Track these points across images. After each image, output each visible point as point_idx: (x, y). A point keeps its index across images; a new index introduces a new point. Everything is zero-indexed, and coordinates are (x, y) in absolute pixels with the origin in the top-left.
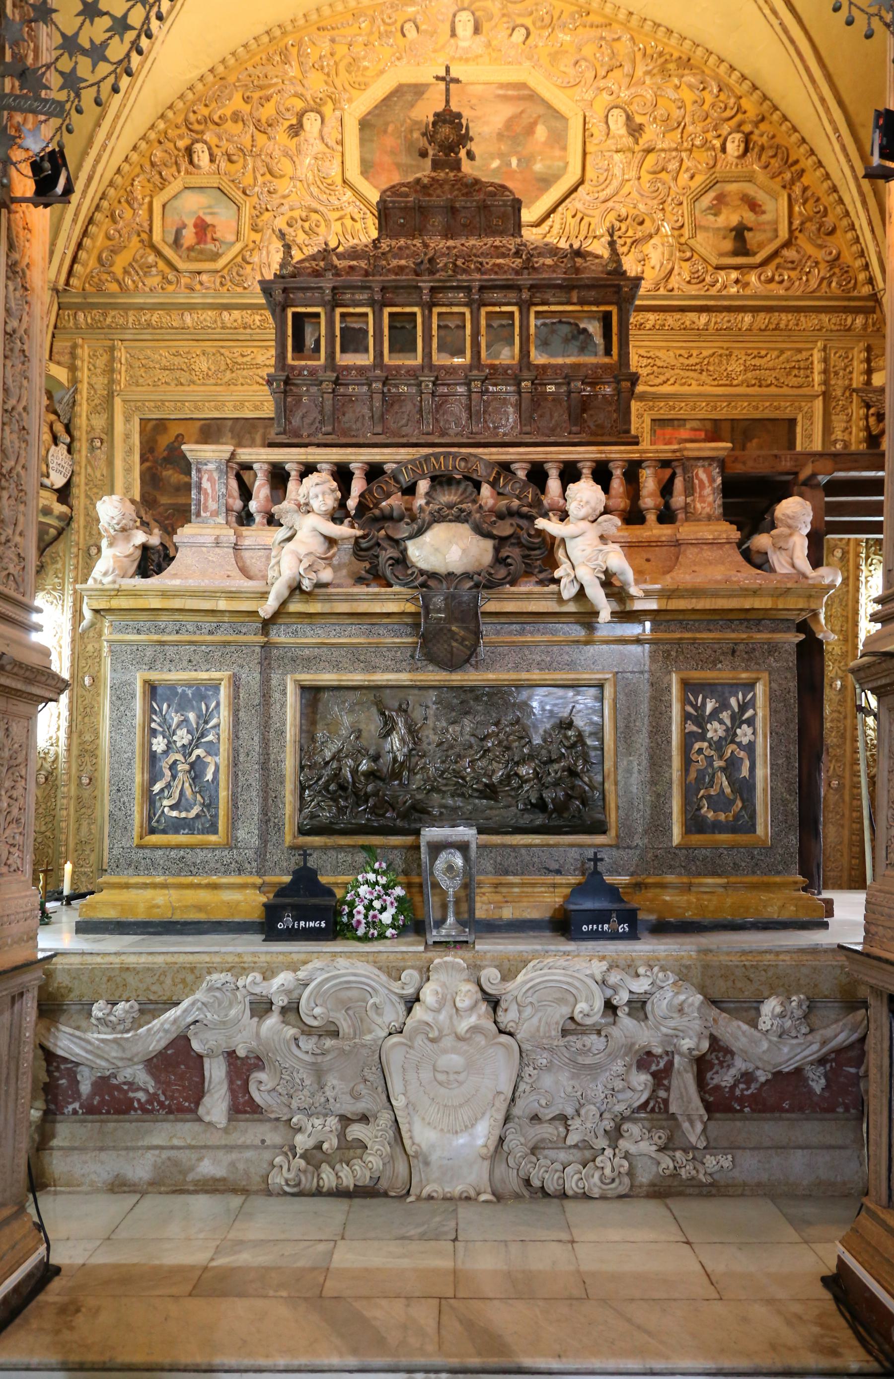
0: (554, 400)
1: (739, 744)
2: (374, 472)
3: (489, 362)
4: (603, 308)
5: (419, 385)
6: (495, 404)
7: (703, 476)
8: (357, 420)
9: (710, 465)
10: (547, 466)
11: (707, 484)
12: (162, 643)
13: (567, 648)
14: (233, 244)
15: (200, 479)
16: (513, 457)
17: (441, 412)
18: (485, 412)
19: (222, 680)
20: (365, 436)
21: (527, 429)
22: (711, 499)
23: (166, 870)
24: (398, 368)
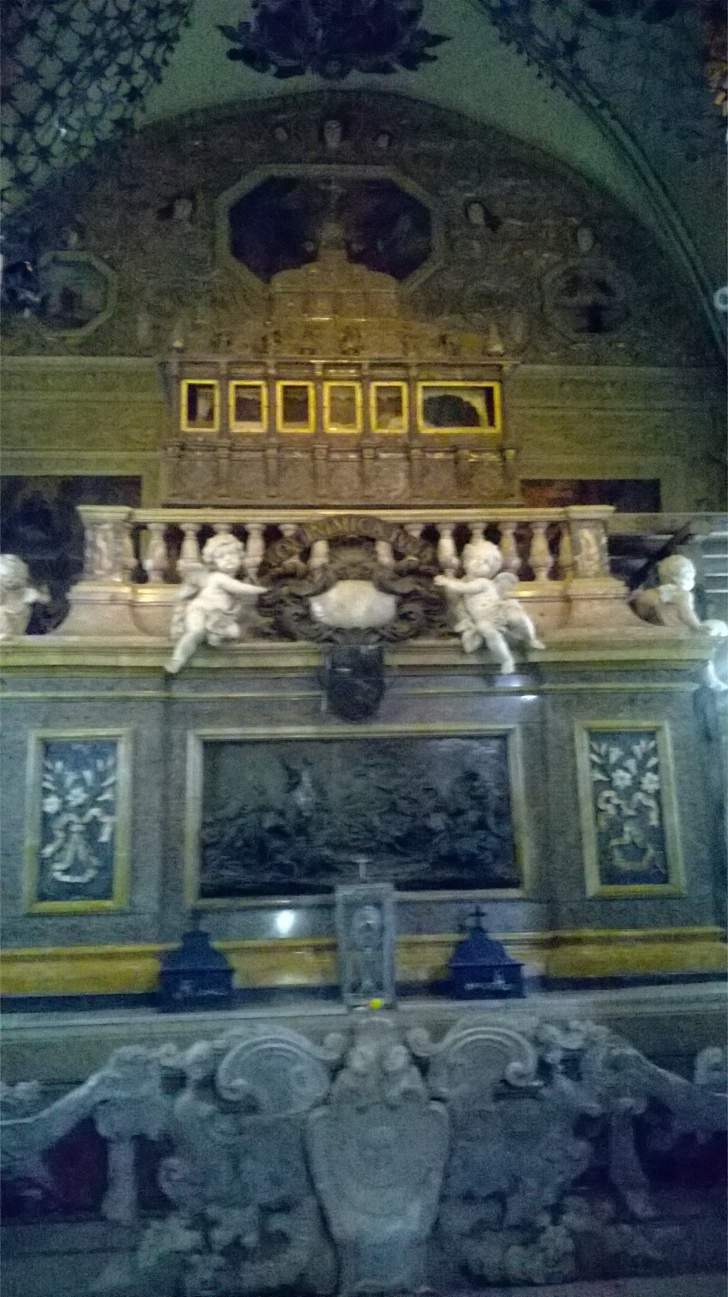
1: (646, 792)
2: (272, 534)
5: (313, 451)
10: (439, 527)
15: (95, 537)
16: (407, 519)
19: (120, 736)
22: (597, 557)
23: (56, 942)
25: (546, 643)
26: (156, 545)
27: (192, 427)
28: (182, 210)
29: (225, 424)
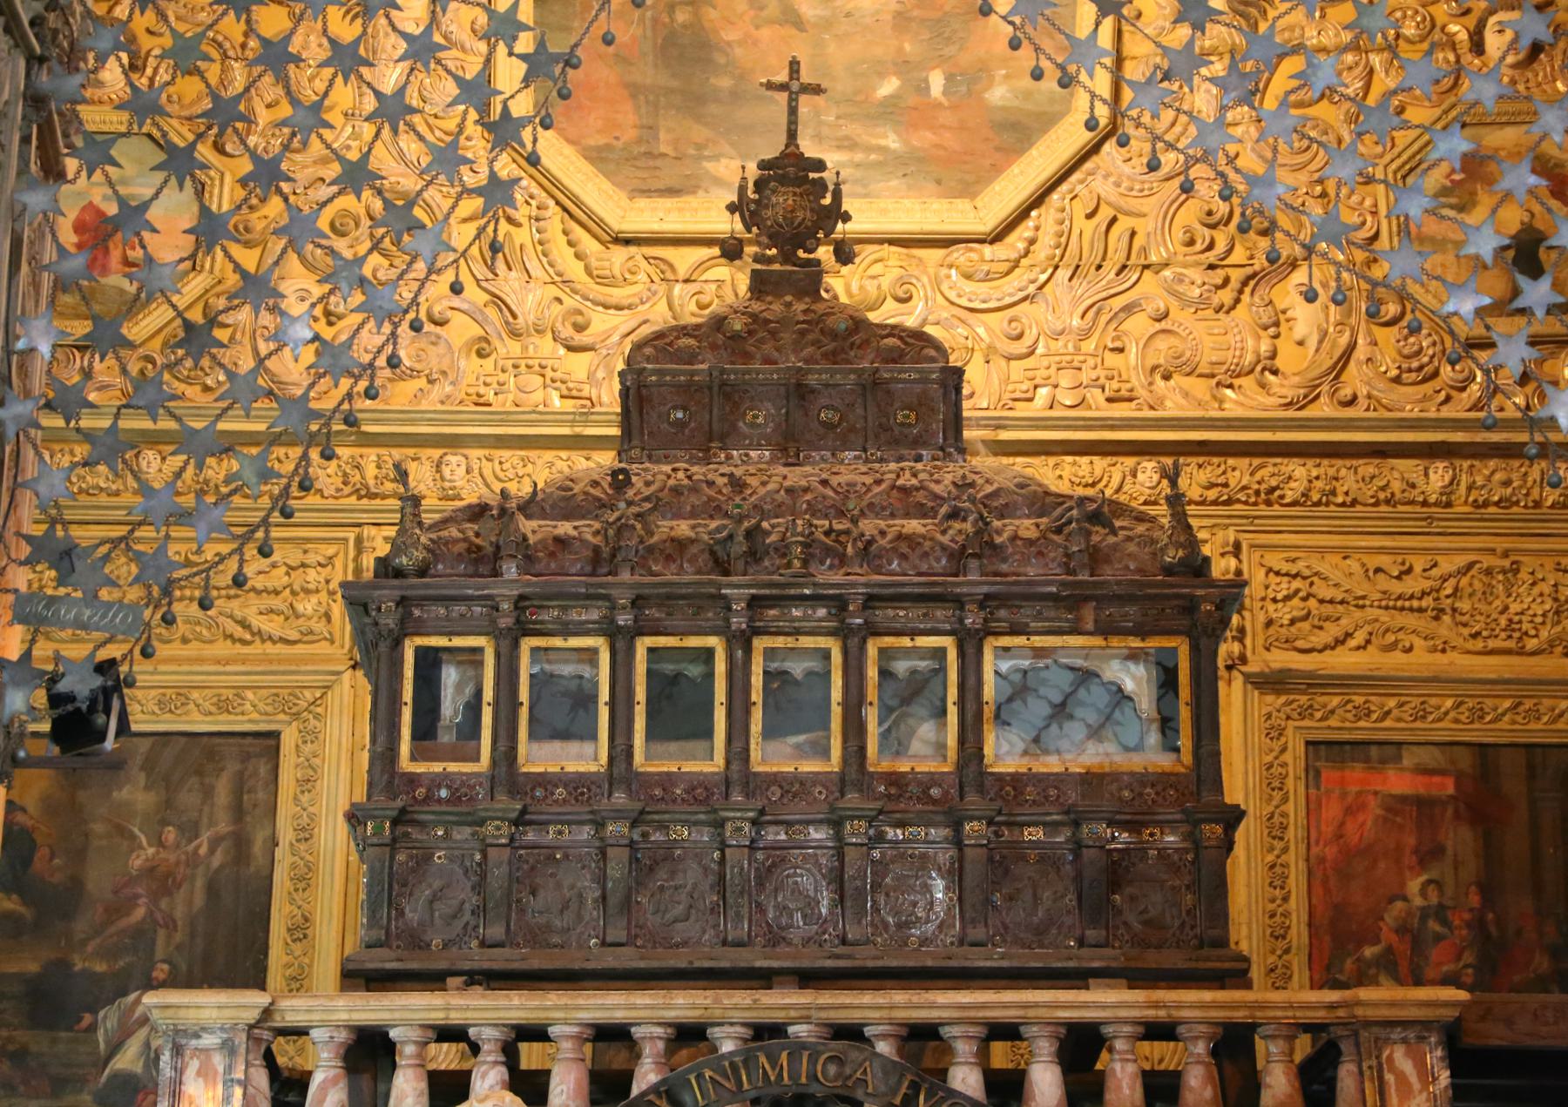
0: (1042, 859)
3: (885, 766)
4: (1154, 643)
5: (720, 824)
6: (896, 868)
7: (1405, 1065)
8: (565, 907)
9: (1421, 1039)
11: (1416, 1085)
16: (945, 1014)
17: (769, 887)
18: (876, 886)
20: (583, 945)
21: (978, 933)
24: (667, 780)
29: (506, 754)
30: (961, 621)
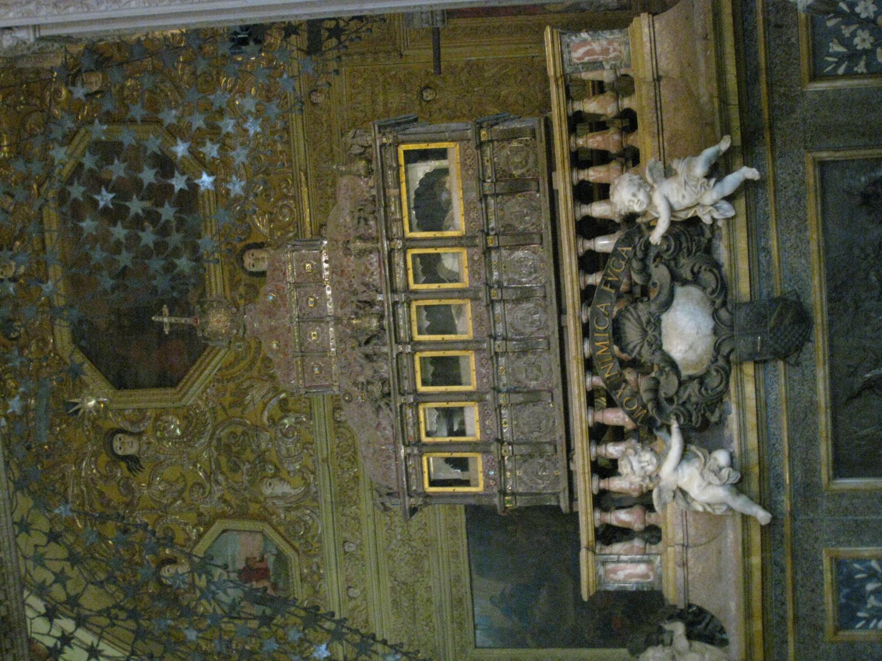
7: (581, 51)
10: (578, 217)
11: (588, 48)
12: (796, 619)
13: (782, 203)
14: (265, 538)
25: (722, 135)
26: (617, 519)
27: (477, 479)
28: (126, 446)
29: (473, 446)
30: (399, 250)
